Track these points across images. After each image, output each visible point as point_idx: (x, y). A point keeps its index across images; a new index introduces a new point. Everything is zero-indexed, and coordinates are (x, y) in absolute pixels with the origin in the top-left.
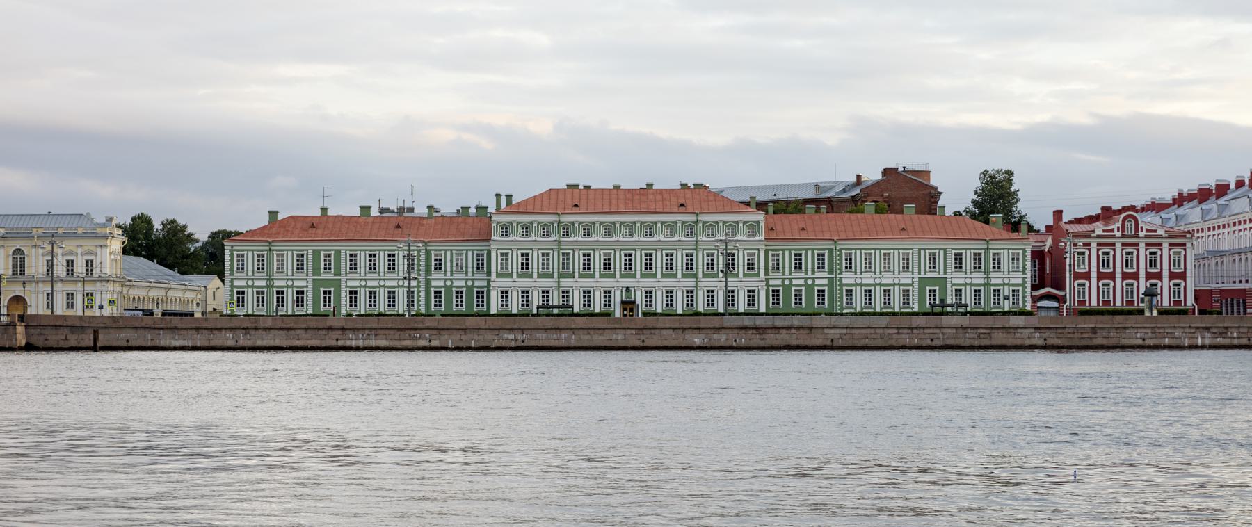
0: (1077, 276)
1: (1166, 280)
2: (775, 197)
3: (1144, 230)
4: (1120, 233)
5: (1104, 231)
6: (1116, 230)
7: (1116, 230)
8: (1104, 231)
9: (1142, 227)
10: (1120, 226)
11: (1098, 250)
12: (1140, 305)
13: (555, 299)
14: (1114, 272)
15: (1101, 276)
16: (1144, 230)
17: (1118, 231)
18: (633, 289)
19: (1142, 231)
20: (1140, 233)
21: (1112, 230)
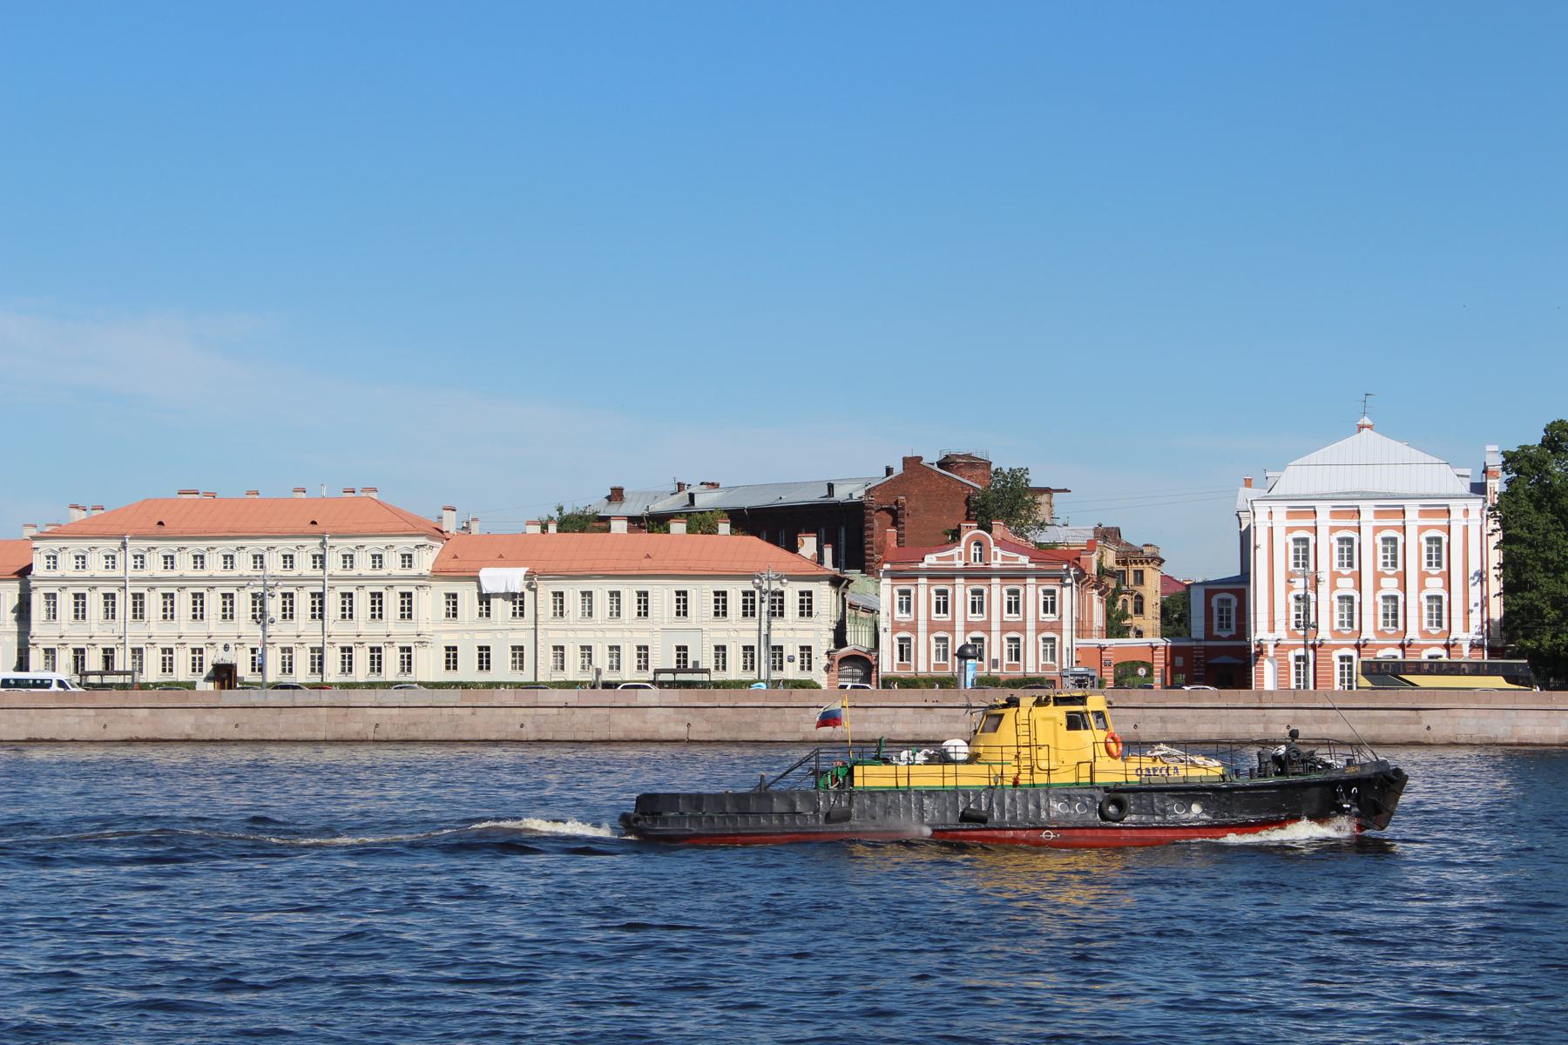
0: (896, 627)
1: (1031, 634)
2: (780, 501)
3: (999, 557)
4: (963, 562)
5: (938, 559)
6: (956, 557)
7: (956, 557)
8: (938, 559)
9: (996, 553)
10: (963, 551)
11: (929, 586)
12: (993, 670)
13: (122, 661)
14: (989, 621)
15: (932, 627)
16: (999, 557)
17: (960, 558)
18: (232, 647)
19: (996, 559)
20: (993, 561)
21: (952, 558)
